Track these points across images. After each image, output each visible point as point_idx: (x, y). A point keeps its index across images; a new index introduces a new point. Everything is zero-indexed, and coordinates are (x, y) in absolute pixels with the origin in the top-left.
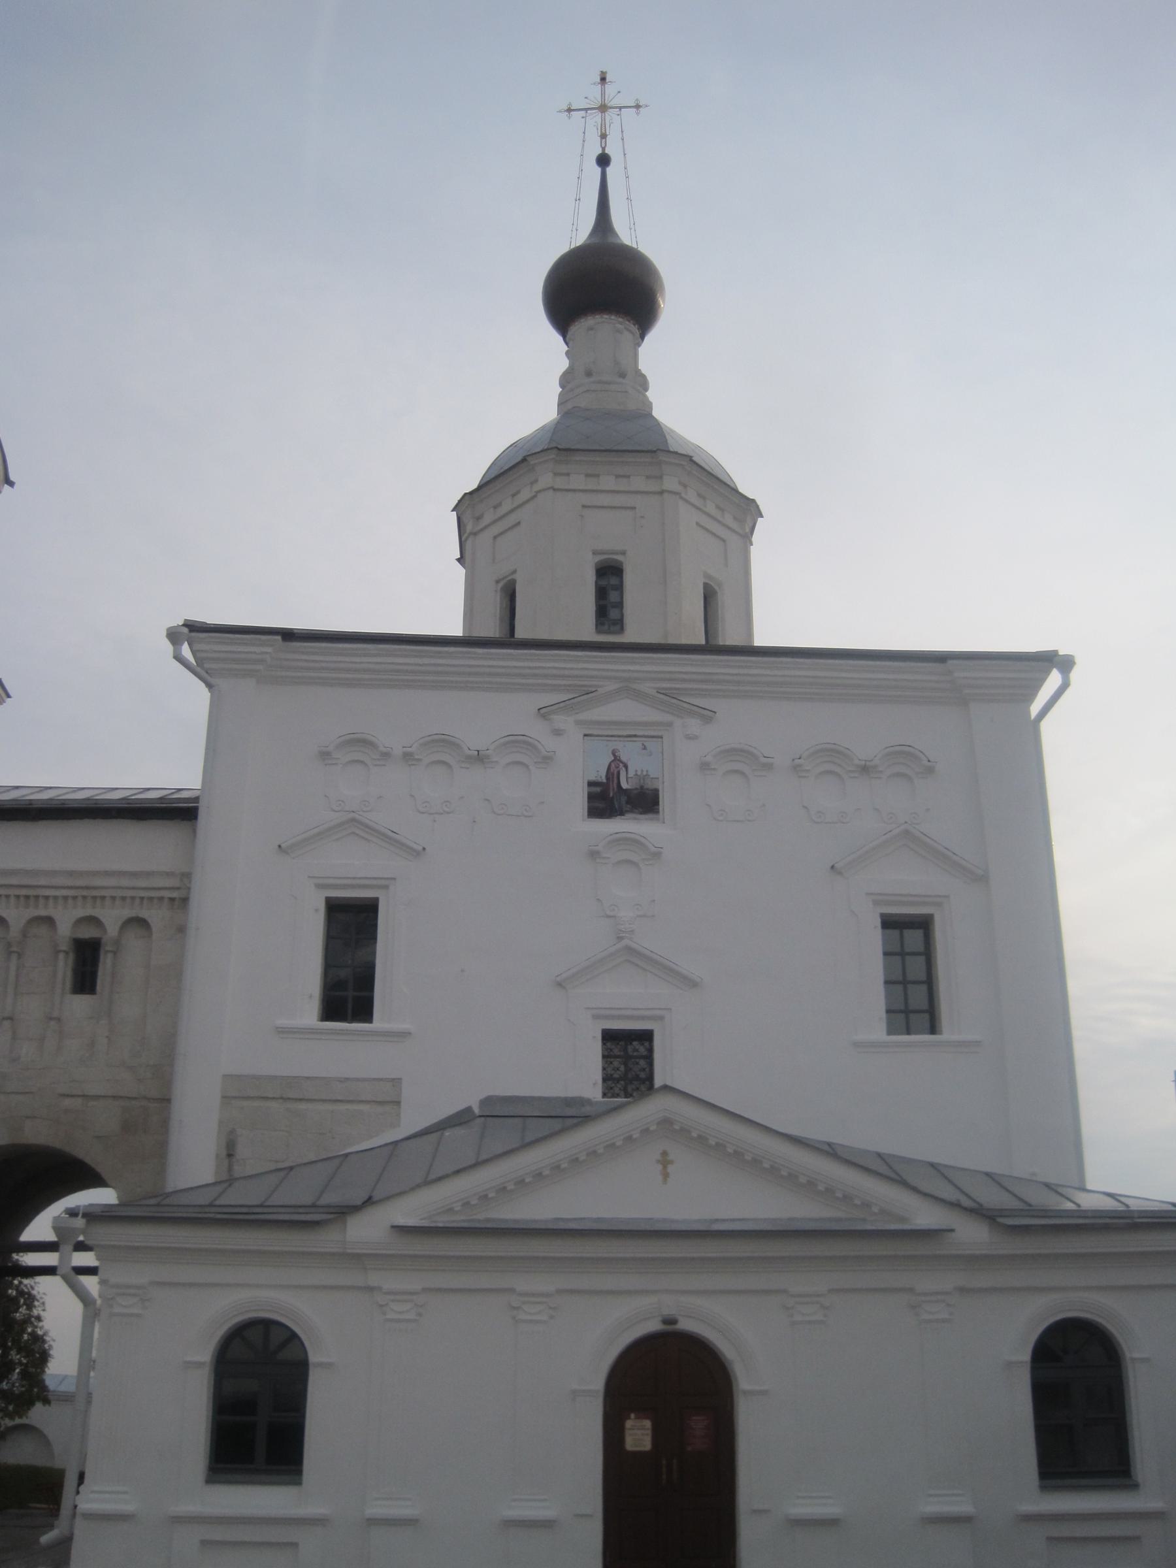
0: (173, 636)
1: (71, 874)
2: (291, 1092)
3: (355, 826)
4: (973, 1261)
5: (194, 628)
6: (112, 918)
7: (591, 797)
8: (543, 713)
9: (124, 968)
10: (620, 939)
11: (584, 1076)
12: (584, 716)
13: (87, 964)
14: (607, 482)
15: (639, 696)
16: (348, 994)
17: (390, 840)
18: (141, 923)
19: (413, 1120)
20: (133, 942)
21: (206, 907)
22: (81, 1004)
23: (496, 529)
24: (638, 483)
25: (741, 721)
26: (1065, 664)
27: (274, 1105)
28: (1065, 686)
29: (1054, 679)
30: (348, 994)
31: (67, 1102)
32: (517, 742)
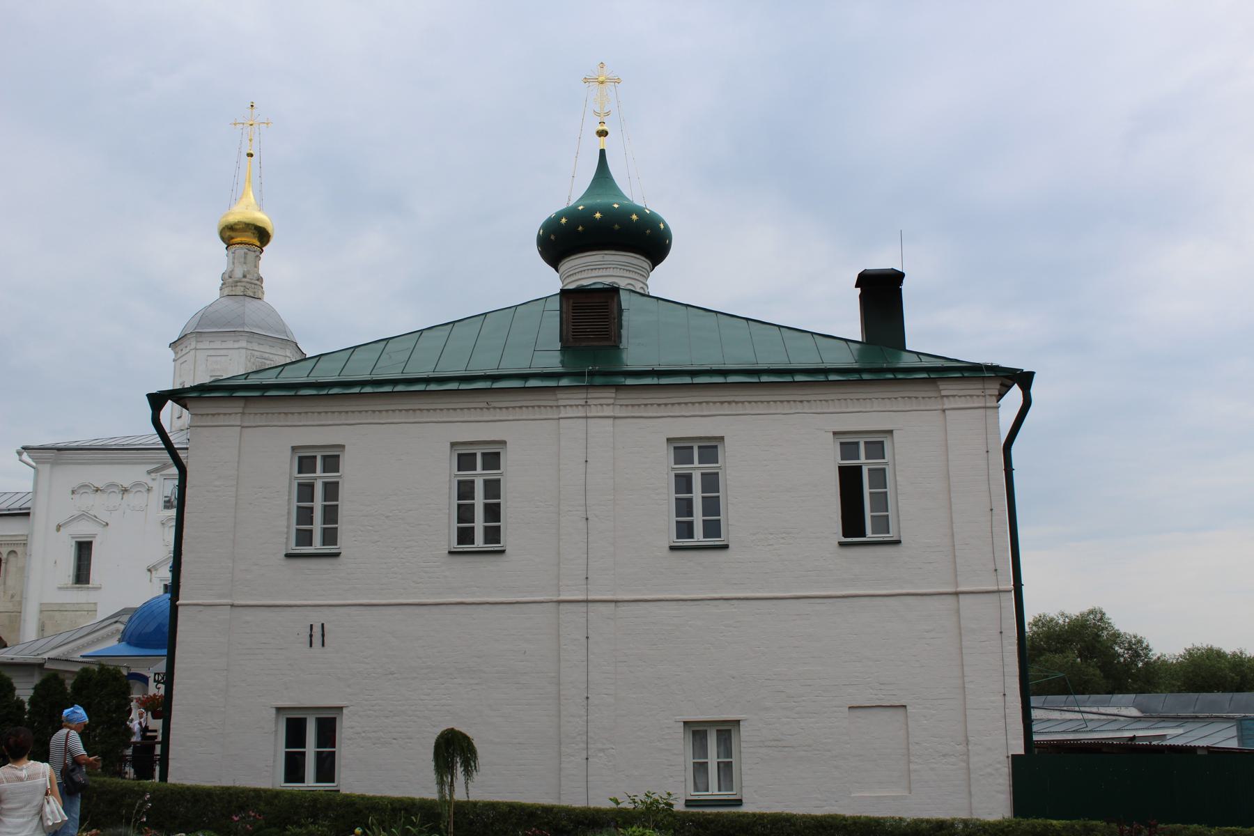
0: (20, 454)
2: (61, 608)
3: (83, 516)
5: (25, 448)
8: (149, 472)
14: (217, 345)
16: (82, 575)
18: (14, 552)
19: (101, 616)
20: (12, 558)
21: (37, 546)
24: (230, 344)
30: (82, 575)
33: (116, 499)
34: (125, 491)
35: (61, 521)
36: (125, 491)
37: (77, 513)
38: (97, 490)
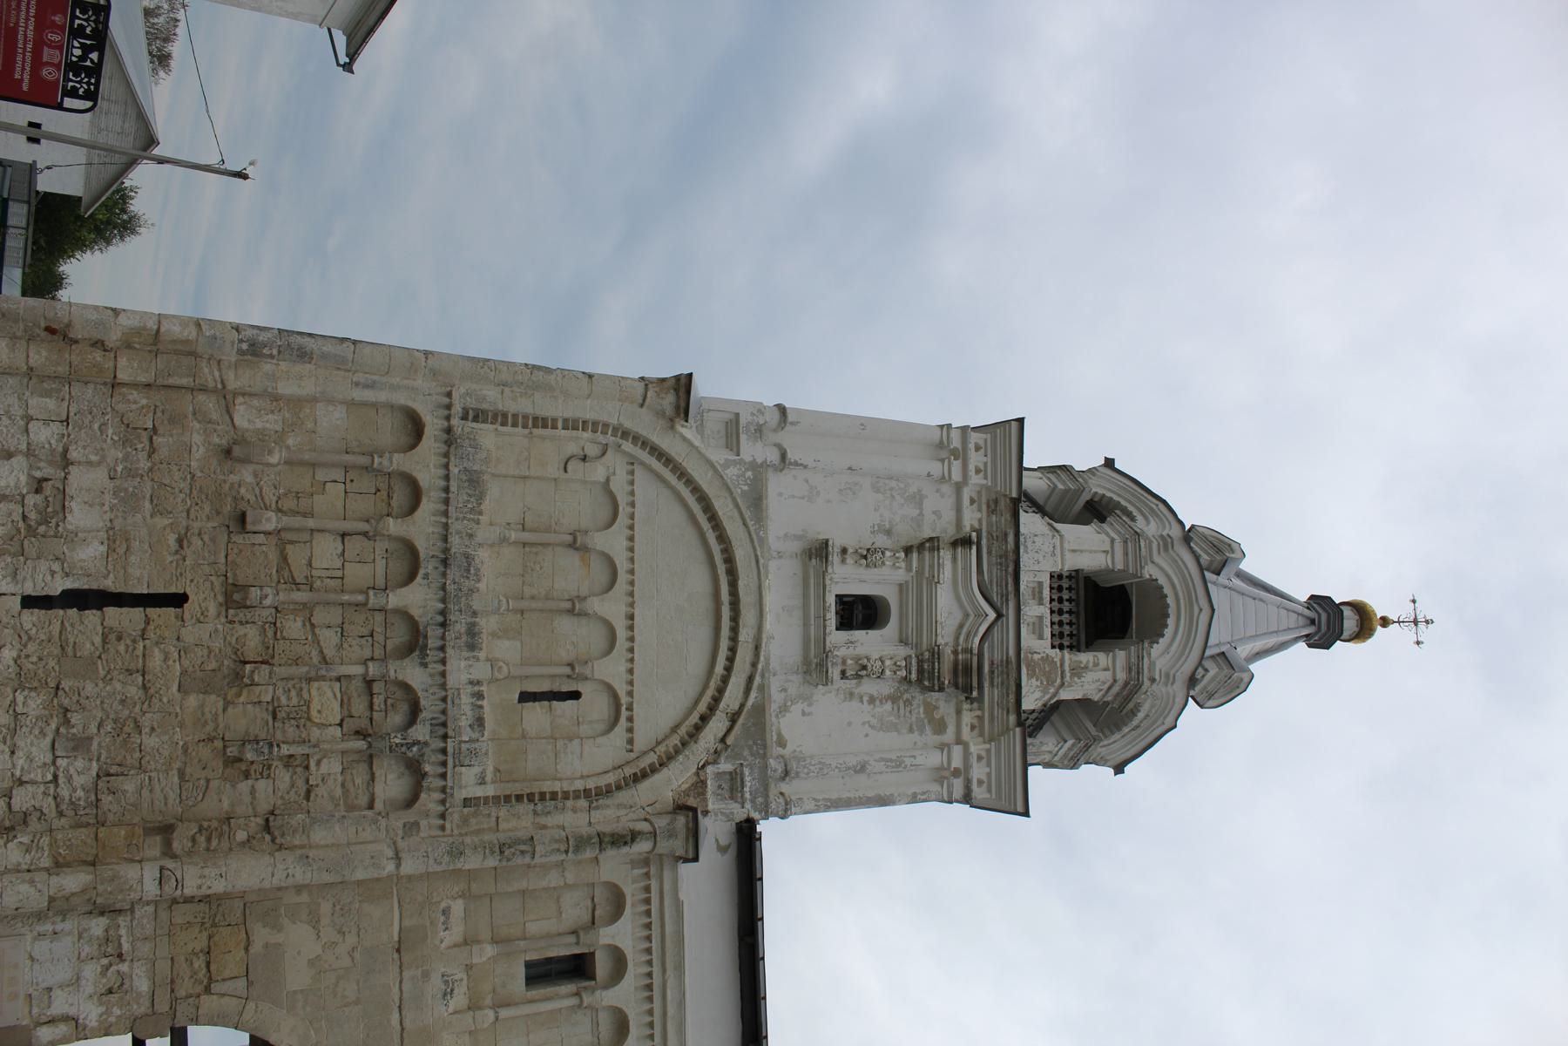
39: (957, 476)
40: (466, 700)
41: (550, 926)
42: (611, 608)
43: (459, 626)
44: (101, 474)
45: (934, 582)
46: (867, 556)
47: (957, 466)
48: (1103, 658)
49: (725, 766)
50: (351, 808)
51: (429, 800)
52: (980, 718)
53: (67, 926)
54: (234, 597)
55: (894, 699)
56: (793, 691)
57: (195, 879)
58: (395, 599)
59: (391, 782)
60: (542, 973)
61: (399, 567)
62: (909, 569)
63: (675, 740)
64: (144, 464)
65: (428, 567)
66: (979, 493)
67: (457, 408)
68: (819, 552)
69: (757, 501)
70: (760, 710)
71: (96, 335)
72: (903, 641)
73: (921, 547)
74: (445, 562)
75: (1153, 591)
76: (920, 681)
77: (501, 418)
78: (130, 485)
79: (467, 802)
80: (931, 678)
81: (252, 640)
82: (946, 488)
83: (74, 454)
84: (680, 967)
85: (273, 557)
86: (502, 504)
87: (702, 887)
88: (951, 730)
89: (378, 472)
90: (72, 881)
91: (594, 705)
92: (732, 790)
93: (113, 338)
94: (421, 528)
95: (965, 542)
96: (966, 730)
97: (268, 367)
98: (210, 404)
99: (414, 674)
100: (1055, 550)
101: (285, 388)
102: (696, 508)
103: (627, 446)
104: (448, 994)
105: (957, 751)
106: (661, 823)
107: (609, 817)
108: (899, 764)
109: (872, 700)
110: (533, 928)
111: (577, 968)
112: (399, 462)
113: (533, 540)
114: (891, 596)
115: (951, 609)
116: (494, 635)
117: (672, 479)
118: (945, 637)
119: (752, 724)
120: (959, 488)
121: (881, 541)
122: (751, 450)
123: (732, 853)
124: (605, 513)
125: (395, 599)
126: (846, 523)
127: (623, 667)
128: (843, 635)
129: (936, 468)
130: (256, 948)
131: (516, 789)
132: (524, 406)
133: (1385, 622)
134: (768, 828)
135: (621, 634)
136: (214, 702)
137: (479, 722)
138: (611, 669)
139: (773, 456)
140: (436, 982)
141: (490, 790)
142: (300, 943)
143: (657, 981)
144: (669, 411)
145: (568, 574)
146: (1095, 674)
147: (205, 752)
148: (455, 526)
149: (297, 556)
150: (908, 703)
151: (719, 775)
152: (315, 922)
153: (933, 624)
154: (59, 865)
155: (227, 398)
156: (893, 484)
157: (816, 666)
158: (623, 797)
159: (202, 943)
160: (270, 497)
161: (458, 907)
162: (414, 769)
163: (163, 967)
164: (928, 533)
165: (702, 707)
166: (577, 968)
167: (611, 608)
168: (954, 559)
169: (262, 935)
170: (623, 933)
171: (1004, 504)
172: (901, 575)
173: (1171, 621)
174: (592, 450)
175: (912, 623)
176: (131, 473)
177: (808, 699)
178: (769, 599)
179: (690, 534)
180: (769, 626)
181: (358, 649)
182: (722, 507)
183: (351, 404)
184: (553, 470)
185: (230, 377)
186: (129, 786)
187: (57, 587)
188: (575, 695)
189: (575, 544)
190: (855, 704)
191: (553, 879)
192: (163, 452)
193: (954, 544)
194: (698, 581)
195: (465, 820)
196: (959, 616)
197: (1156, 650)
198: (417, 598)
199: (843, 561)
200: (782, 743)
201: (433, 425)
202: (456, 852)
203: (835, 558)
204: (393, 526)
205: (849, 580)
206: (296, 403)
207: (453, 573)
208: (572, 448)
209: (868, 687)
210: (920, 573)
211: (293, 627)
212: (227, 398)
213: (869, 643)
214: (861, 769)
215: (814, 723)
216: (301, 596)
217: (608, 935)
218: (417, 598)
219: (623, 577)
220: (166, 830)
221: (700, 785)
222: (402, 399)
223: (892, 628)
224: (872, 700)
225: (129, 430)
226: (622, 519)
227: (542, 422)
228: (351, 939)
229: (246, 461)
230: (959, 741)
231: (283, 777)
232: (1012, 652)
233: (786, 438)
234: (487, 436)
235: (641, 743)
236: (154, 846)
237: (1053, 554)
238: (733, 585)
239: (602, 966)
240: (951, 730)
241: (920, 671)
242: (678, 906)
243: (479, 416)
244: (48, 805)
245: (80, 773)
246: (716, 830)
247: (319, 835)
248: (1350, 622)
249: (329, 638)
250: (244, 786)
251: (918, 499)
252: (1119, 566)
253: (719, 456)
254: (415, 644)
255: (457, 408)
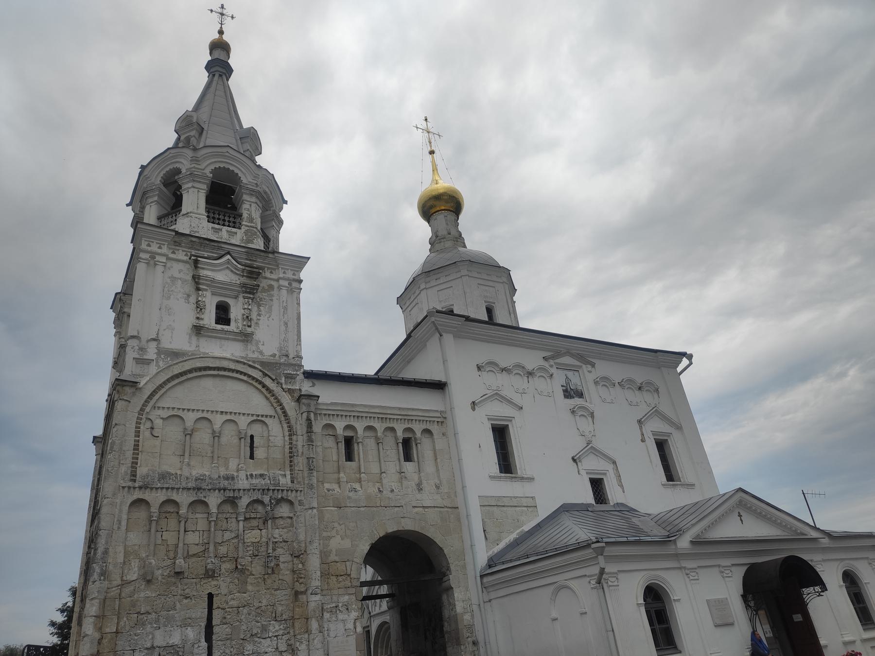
1: (400, 409)
3: (498, 396)
4: (825, 550)
6: (418, 428)
7: (564, 391)
9: (424, 449)
10: (588, 444)
11: (587, 496)
12: (557, 361)
13: (407, 447)
15: (572, 356)
16: (506, 464)
17: (509, 402)
19: (543, 513)
22: (409, 467)
23: (437, 288)
25: (603, 368)
26: (690, 357)
27: (495, 508)
28: (691, 363)
29: (685, 362)
30: (506, 464)
31: (416, 510)
32: (542, 369)
33: (520, 382)
34: (530, 374)
35: (476, 397)
36: (530, 374)
37: (490, 393)
38: (503, 370)
39: (164, 259)
40: (254, 481)
41: (334, 451)
42: (218, 420)
43: (226, 483)
44: (158, 633)
45: (213, 281)
46: (200, 307)
47: (158, 258)
48: (246, 206)
49: (283, 380)
50: (292, 525)
51: (291, 496)
52: (268, 268)
53: (326, 626)
54: (210, 574)
55: (259, 306)
56: (254, 348)
57: (316, 583)
58: (214, 510)
59: (284, 510)
60: (349, 457)
61: (200, 508)
62: (206, 290)
63: (272, 399)
64: (153, 616)
65: (201, 496)
66: (170, 249)
67: (130, 484)
68: (198, 330)
69: (175, 354)
70: (263, 363)
71: (96, 643)
72: (236, 297)
73: (197, 283)
74: (199, 489)
75: (215, 171)
76: (253, 294)
77: (134, 464)
78: (162, 620)
79: (292, 482)
80: (254, 289)
81: (227, 566)
82: (168, 265)
83: (149, 645)
84: (353, 405)
85: (194, 559)
86: (171, 464)
87: (328, 394)
88: (272, 283)
89: (159, 518)
90: (314, 625)
91: (257, 430)
92: (291, 378)
93: (97, 636)
94: (184, 499)
95: (196, 262)
96: (273, 276)
97: (111, 567)
98: (127, 590)
99: (244, 501)
100: (194, 216)
101: (121, 559)
102: (177, 381)
103: (148, 409)
104: (355, 490)
105: (282, 282)
106: (304, 408)
107: (300, 428)
108: (285, 308)
109: (259, 315)
110: (335, 458)
111: (349, 442)
112: (154, 509)
113: (185, 451)
114: (217, 299)
115: (223, 274)
116: (227, 469)
117: (163, 390)
118: (236, 279)
119: (268, 367)
120: (168, 259)
121: (193, 299)
122: (151, 353)
123: (316, 382)
124: (177, 420)
125: (214, 510)
126: (185, 316)
127: (243, 418)
128: (232, 323)
129: (160, 268)
130: (337, 559)
131: (287, 462)
132: (129, 454)
133: (221, 32)
134: (309, 365)
135: (229, 417)
136: (250, 579)
137: (261, 475)
138: (243, 422)
139: (153, 345)
140: (351, 494)
141: (288, 473)
142: (336, 543)
143: (356, 414)
144: (133, 390)
145: (203, 437)
146: (250, 209)
147: (269, 581)
148: (184, 485)
149: (194, 550)
150: (261, 299)
151: (286, 383)
152: (330, 538)
153: (230, 284)
154: (308, 631)
155: (125, 583)
156: (166, 289)
157: (245, 337)
158: (293, 422)
159: (334, 578)
160: (169, 562)
161: (327, 486)
162: (279, 501)
163: (341, 591)
164: (189, 278)
165: (260, 387)
166: (349, 442)
167: (218, 420)
168: (203, 269)
169: (333, 557)
170: (339, 425)
171: (177, 239)
172: (208, 294)
173: (231, 168)
174: (149, 425)
175: (228, 293)
176: (157, 621)
177: (258, 342)
178: (218, 353)
179: (187, 385)
180: (228, 356)
181: (233, 524)
182: (177, 370)
183: (127, 530)
184: (157, 442)
185: (115, 583)
186: (280, 609)
187: (204, 644)
188: (252, 437)
189: (189, 434)
190: (260, 322)
191: (320, 450)
192: (148, 608)
193: (196, 267)
194: (208, 383)
195: (299, 483)
196: (228, 271)
197: (244, 180)
198: (214, 500)
199: (202, 319)
200: (274, 355)
201: (137, 495)
202: (311, 487)
203: (201, 322)
204: (183, 511)
205: (209, 318)
206: (126, 554)
207: (204, 486)
208: (147, 434)
209: (254, 316)
210: (208, 285)
211: (223, 550)
212: (125, 583)
213: (236, 312)
214: (286, 324)
215: (268, 341)
216: (212, 548)
217: (340, 431)
218: (214, 500)
219: (205, 415)
220: (297, 594)
221: (290, 391)
222: (126, 508)
223: (231, 302)
224: (259, 315)
225: (139, 624)
226: (180, 413)
227: (136, 447)
228: (336, 525)
229: (153, 573)
230: (278, 280)
231: (279, 551)
232: (243, 250)
233: (144, 337)
234: (142, 471)
235: (271, 412)
236: (303, 598)
237: (199, 219)
238: (210, 368)
239: (349, 433)
240: (272, 283)
241: (249, 293)
242: (332, 404)
243: (134, 475)
244: (285, 638)
245: (275, 628)
246: (307, 387)
247: (302, 537)
248: (219, 54)
249: (228, 535)
250: (282, 566)
251: (173, 279)
252: (205, 187)
253: (153, 369)
254: (232, 501)
255: (130, 484)
